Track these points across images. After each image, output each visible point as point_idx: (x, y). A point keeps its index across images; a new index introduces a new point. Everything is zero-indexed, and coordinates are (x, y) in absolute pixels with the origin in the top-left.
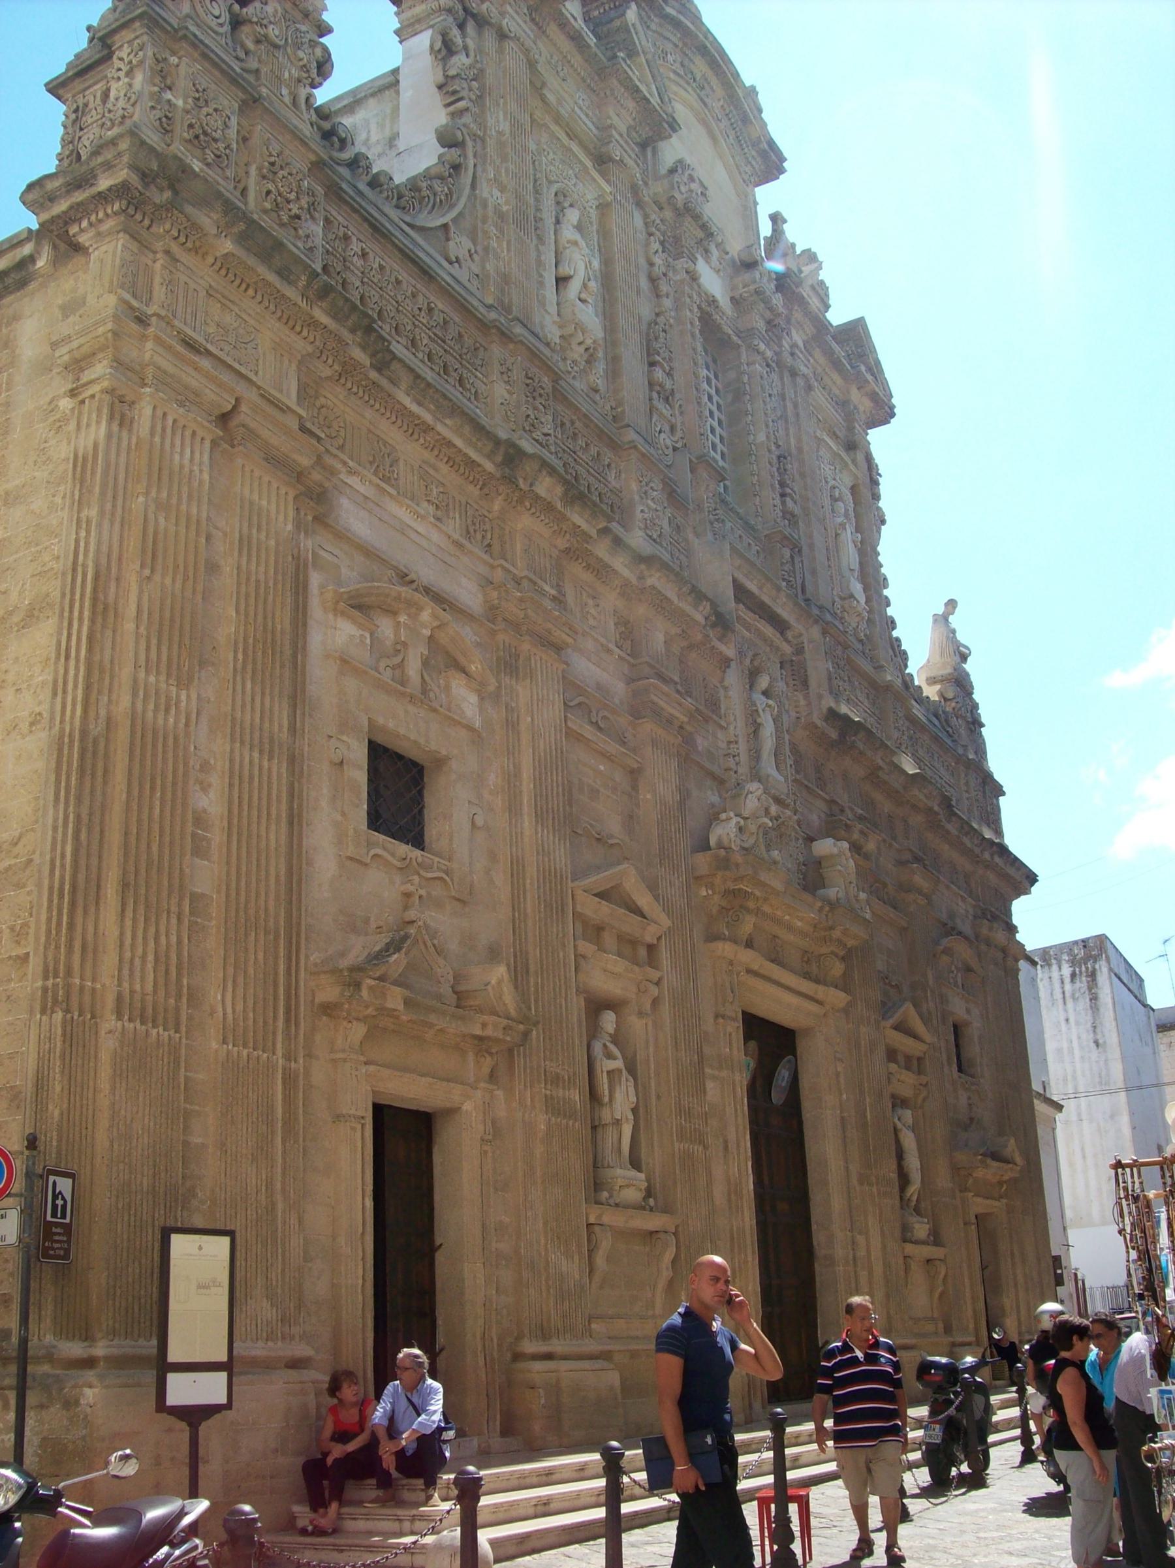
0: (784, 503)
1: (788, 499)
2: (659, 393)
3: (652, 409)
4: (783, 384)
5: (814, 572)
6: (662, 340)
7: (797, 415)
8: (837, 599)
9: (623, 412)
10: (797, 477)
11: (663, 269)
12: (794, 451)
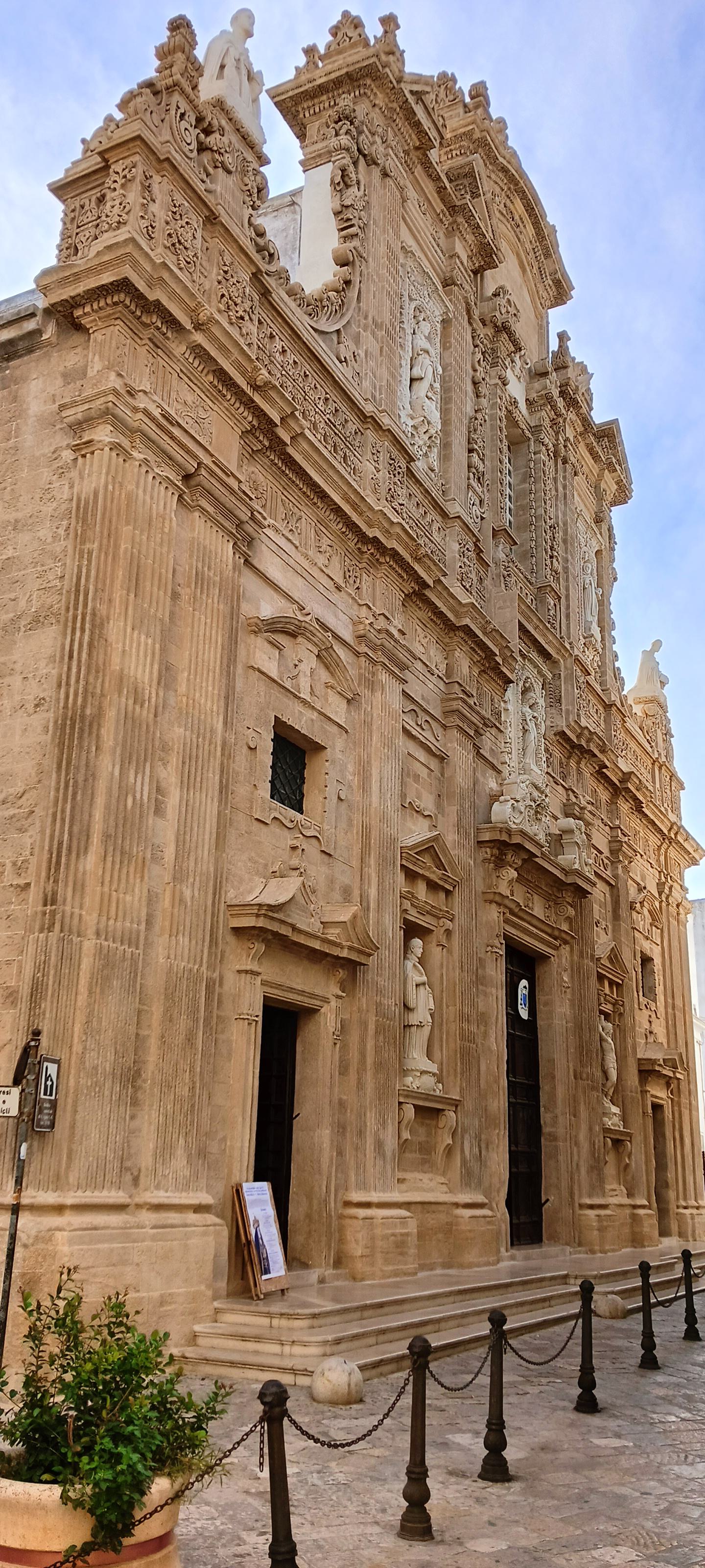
5: (568, 616)
8: (581, 638)
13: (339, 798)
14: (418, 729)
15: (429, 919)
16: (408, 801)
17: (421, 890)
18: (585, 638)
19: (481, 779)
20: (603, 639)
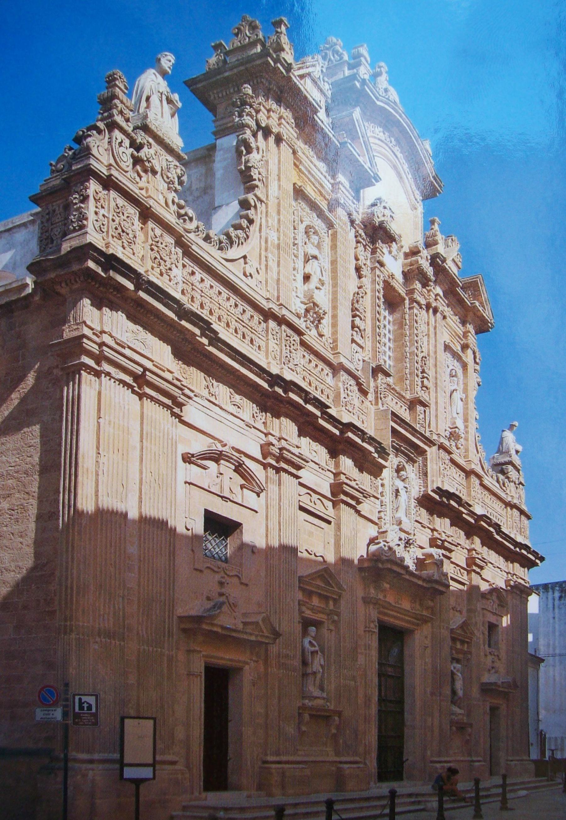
0: (422, 382)
2: (357, 332)
3: (353, 341)
5: (436, 416)
6: (360, 302)
8: (448, 429)
9: (337, 345)
12: (432, 354)
17: (315, 601)
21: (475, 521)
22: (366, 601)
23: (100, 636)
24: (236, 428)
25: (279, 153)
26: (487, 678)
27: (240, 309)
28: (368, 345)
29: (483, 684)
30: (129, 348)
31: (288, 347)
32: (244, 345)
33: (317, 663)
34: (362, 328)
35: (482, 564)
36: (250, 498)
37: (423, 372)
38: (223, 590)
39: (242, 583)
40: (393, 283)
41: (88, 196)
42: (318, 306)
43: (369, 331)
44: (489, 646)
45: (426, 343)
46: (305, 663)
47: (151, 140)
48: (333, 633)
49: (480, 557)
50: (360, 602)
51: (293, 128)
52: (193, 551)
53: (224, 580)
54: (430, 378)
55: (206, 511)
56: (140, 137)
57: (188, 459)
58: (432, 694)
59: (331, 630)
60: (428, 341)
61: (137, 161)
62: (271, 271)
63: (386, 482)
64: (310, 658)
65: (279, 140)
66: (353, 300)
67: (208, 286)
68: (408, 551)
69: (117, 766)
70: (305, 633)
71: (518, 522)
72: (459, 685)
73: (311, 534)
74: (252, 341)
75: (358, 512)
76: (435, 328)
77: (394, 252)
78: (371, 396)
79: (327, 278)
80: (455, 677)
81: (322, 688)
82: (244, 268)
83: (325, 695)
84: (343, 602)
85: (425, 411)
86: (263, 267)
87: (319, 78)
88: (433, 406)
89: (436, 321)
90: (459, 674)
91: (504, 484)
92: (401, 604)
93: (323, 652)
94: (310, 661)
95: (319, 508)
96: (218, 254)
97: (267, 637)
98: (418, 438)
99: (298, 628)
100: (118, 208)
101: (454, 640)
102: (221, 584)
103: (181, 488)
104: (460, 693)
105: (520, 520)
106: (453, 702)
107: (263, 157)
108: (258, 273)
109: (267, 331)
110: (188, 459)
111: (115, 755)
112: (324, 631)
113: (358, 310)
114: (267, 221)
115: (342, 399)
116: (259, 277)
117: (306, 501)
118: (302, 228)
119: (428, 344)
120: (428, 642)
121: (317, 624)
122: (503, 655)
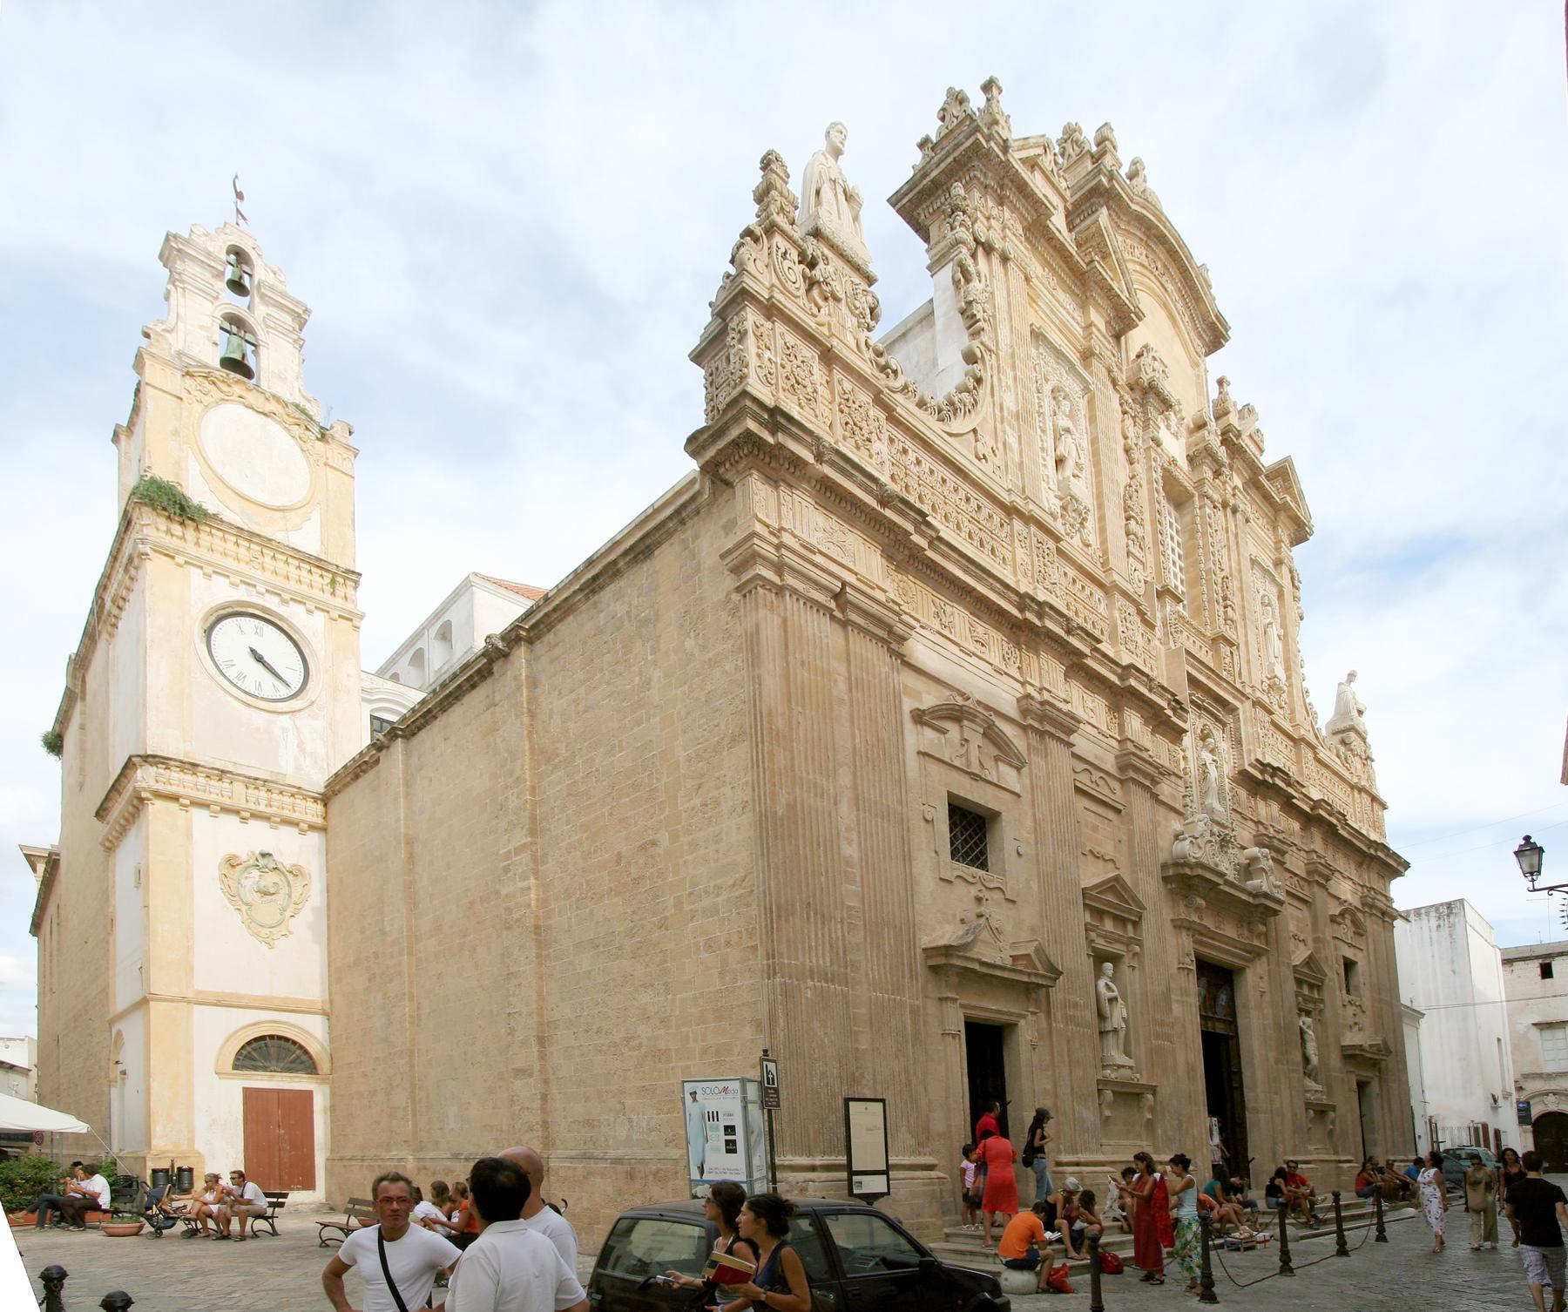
0: (1226, 612)
1: (1229, 609)
3: (1129, 554)
4: (1227, 521)
5: (1248, 661)
6: (1134, 498)
7: (1237, 543)
8: (1265, 679)
10: (1237, 593)
11: (1134, 440)
12: (1235, 573)
13: (1019, 854)
14: (1094, 786)
15: (1118, 946)
16: (1088, 849)
17: (1109, 925)
18: (1269, 679)
19: (1163, 822)
20: (1289, 678)
21: (1312, 809)
22: (1179, 925)
23: (812, 979)
24: (982, 675)
25: (1006, 274)
26: (1351, 1039)
27: (974, 504)
28: (1150, 560)
29: (1343, 1048)
30: (821, 553)
31: (1041, 558)
32: (983, 556)
33: (1118, 1014)
34: (1140, 534)
35: (1327, 872)
36: (1009, 776)
37: (1225, 598)
38: (982, 910)
39: (1007, 900)
40: (1177, 473)
41: (746, 331)
42: (1077, 501)
43: (1149, 540)
44: (1348, 992)
45: (1225, 558)
46: (1101, 1016)
47: (826, 251)
48: (1136, 970)
49: (1323, 861)
50: (1168, 926)
51: (1021, 242)
52: (936, 852)
53: (981, 895)
54: (1236, 607)
55: (948, 792)
56: (813, 247)
57: (919, 717)
58: (1277, 1062)
59: (1134, 968)
60: (1229, 555)
61: (812, 283)
62: (1012, 451)
63: (1189, 754)
64: (1108, 1009)
65: (1005, 259)
66: (1124, 495)
67: (927, 470)
68: (1226, 852)
69: (844, 1175)
70: (1098, 973)
71: (1369, 812)
72: (1311, 1048)
73: (1095, 828)
74: (993, 550)
75: (1155, 797)
76: (1236, 536)
77: (1174, 428)
78: (1159, 632)
79: (1086, 460)
80: (1306, 1036)
81: (1127, 1053)
82: (976, 448)
83: (1131, 1062)
84: (1145, 926)
85: (1232, 653)
86: (1000, 446)
87: (1052, 171)
88: (1242, 646)
89: (1236, 526)
90: (1311, 1032)
91: (1346, 759)
92: (1224, 930)
93: (1125, 1000)
94: (1108, 1012)
95: (1103, 792)
96: (938, 426)
97: (1043, 976)
98: (1225, 689)
99: (1089, 964)
100: (788, 348)
101: (1299, 982)
102: (979, 900)
103: (912, 762)
104: (1315, 1060)
105: (1373, 810)
106: (1308, 1074)
107: (987, 286)
108: (995, 455)
109: (1012, 536)
110: (919, 717)
111: (840, 1157)
112: (1124, 967)
113: (1132, 510)
114: (1000, 379)
115: (1120, 632)
116: (997, 461)
117: (1085, 781)
118: (1047, 389)
119: (1230, 560)
120: (1264, 986)
121: (1115, 959)
122: (1367, 1005)
